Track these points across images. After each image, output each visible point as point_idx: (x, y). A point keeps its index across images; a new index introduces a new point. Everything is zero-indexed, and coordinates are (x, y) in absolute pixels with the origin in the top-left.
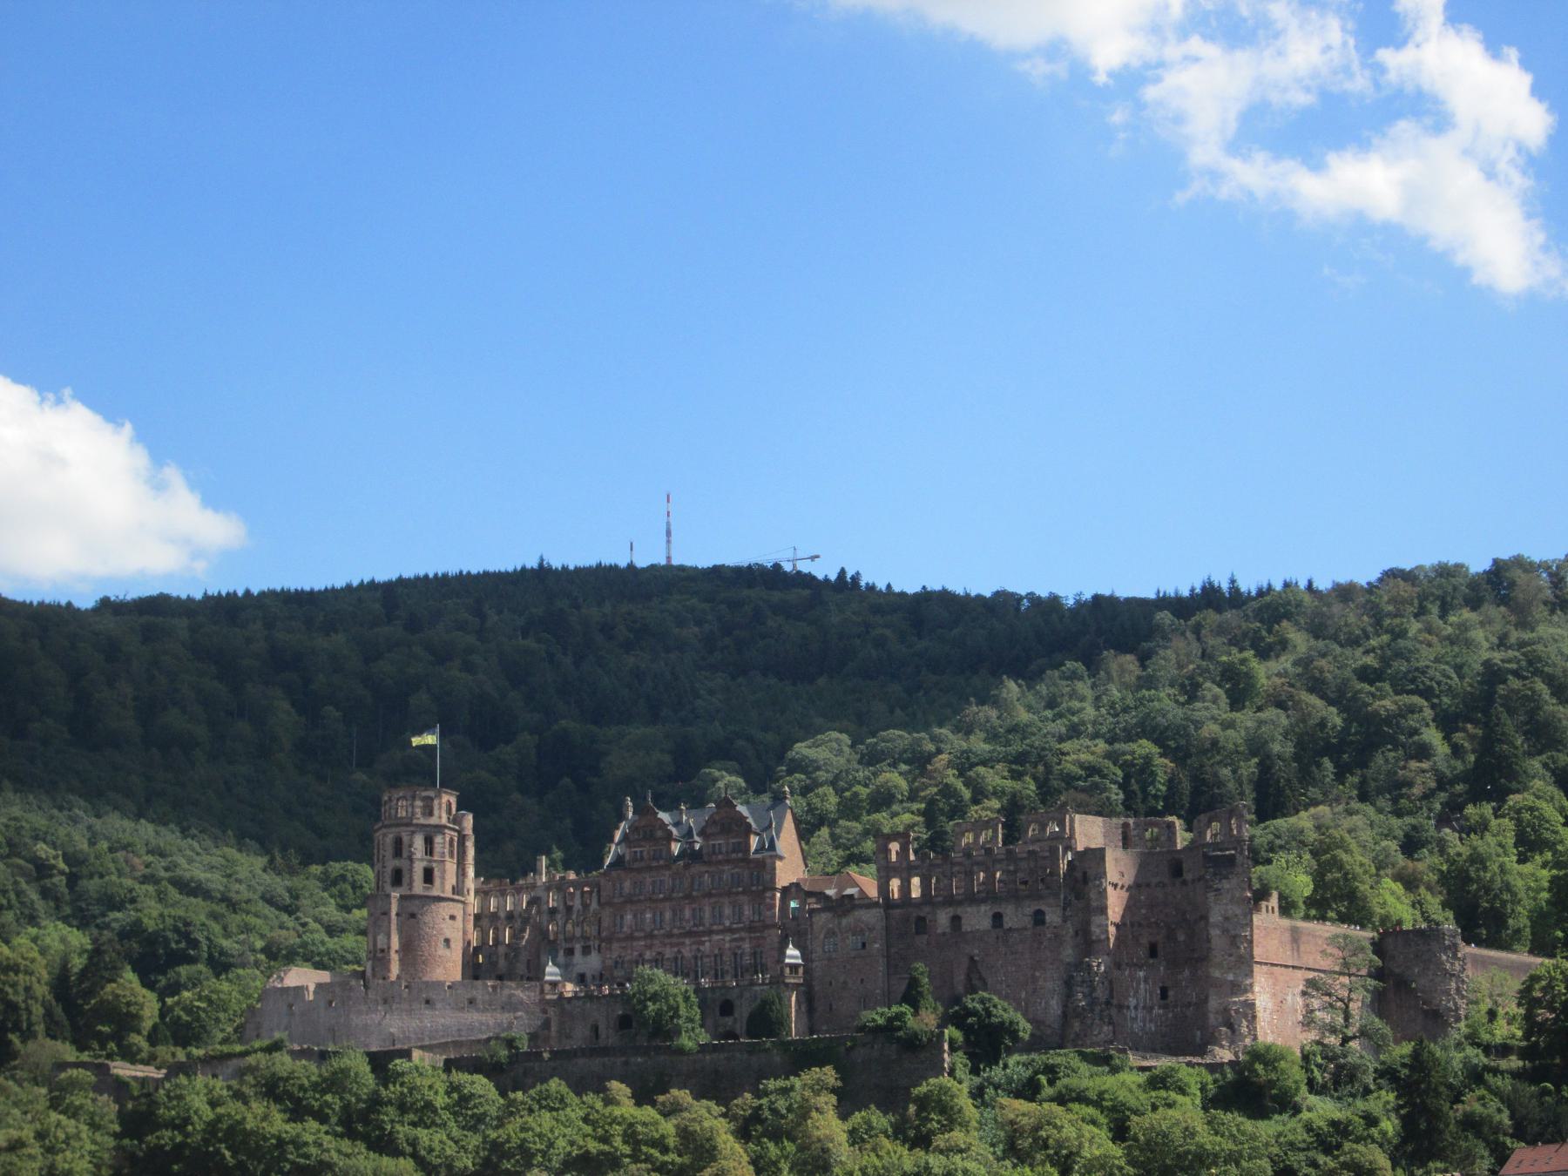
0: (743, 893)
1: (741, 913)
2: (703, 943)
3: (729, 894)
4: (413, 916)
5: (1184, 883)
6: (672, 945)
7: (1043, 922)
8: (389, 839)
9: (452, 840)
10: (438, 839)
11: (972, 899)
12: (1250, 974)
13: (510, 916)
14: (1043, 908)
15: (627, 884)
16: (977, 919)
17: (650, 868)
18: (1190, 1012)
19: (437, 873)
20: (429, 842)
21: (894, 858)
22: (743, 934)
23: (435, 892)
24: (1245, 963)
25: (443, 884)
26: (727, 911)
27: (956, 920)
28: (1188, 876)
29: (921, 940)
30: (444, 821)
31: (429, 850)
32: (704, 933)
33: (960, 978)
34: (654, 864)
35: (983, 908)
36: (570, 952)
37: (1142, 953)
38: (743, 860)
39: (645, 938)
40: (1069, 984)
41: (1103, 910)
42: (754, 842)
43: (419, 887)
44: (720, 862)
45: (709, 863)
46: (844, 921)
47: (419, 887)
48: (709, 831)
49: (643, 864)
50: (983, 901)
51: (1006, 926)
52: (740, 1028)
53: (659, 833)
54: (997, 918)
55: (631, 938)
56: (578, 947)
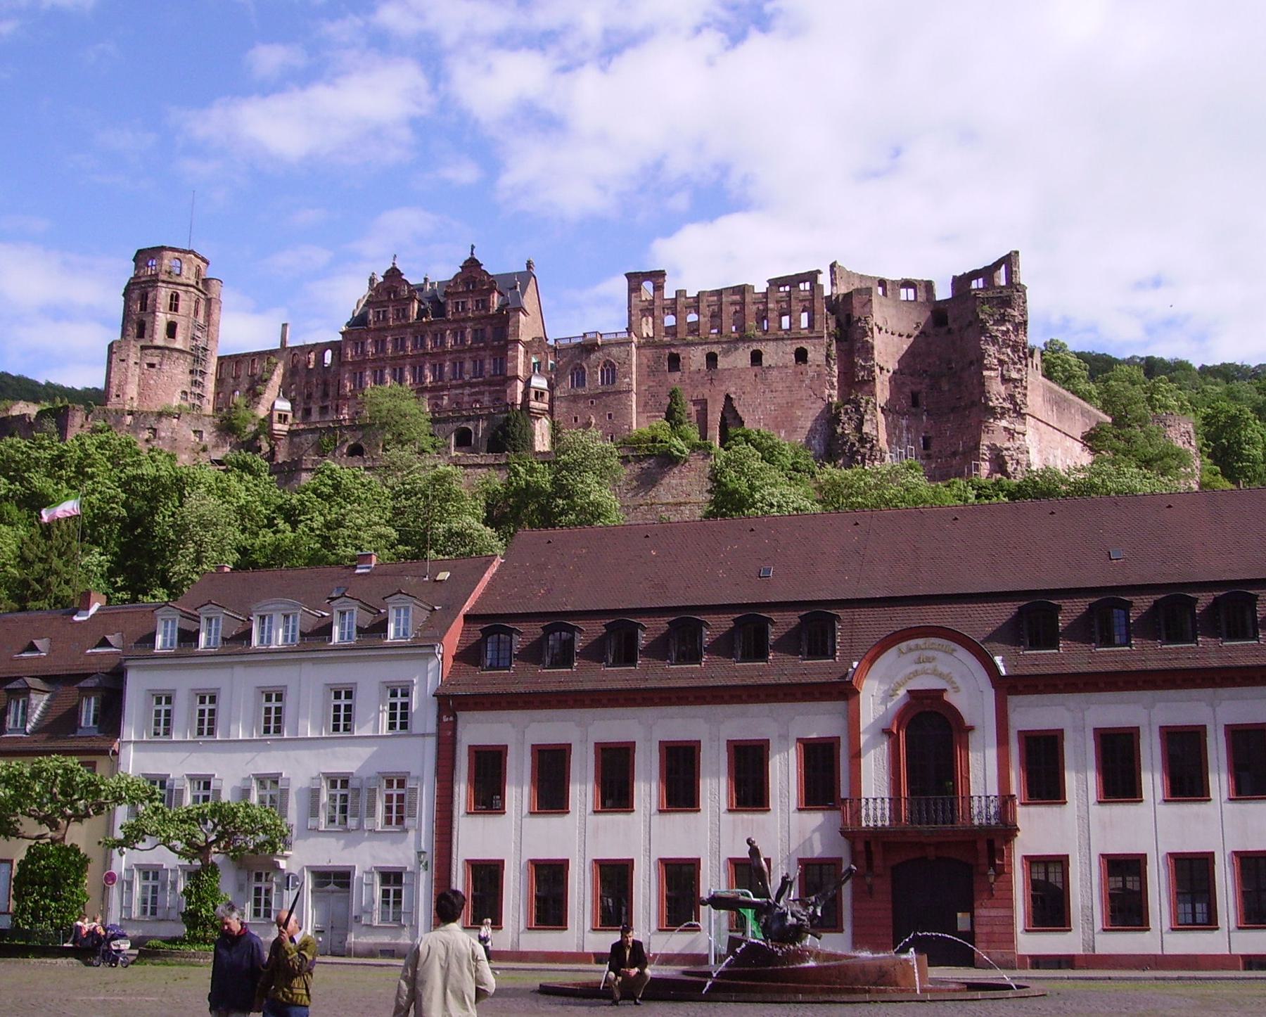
0: (483, 349)
1: (482, 369)
4: (152, 365)
7: (805, 361)
9: (197, 302)
10: (182, 295)
14: (809, 348)
19: (179, 331)
22: (482, 388)
23: (179, 343)
26: (468, 365)
28: (952, 325)
31: (174, 307)
32: (443, 388)
37: (905, 403)
38: (484, 317)
41: (868, 350)
42: (496, 300)
43: (160, 338)
44: (464, 320)
46: (593, 357)
51: (765, 364)
54: (756, 357)
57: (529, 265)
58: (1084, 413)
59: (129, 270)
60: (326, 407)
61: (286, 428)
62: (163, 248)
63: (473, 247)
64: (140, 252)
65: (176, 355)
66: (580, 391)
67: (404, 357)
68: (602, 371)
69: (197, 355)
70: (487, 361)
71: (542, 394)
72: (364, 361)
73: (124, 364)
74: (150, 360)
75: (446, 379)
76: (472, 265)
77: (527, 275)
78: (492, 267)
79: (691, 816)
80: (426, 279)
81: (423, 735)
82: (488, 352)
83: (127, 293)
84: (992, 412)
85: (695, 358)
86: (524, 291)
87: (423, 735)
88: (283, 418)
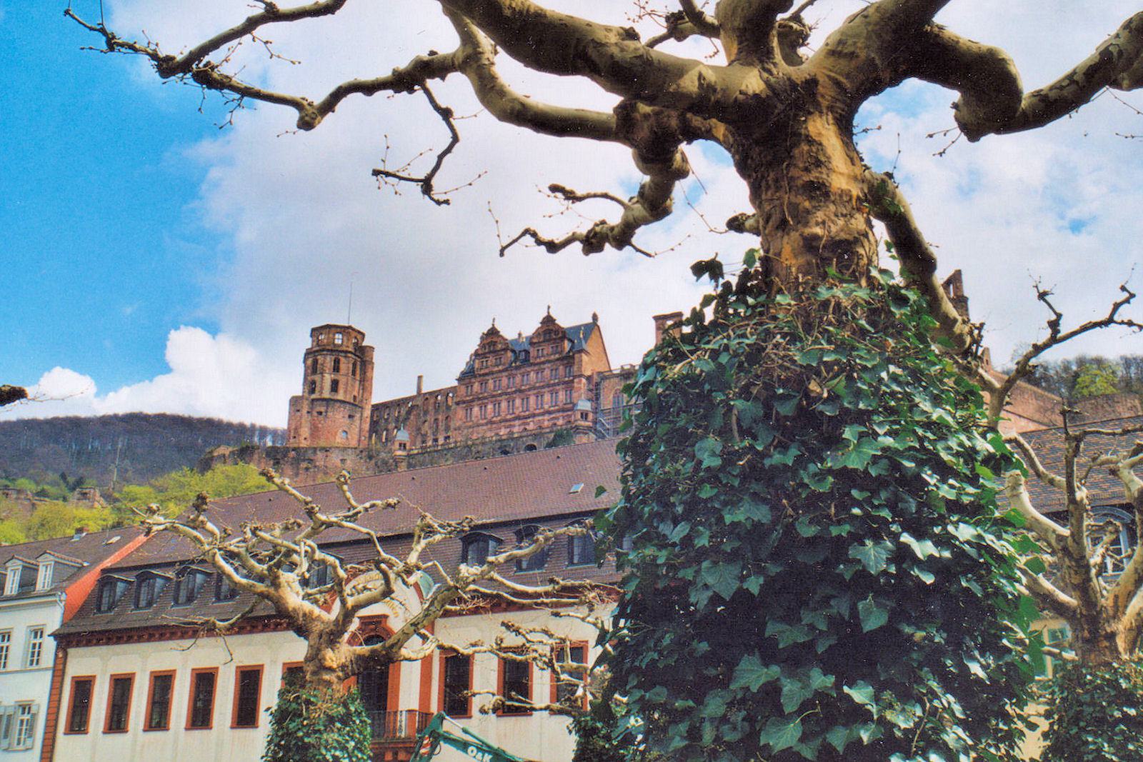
0: (558, 384)
2: (528, 424)
3: (548, 386)
4: (320, 413)
9: (354, 365)
10: (343, 360)
17: (492, 373)
20: (337, 362)
22: (558, 415)
23: (340, 396)
26: (547, 397)
30: (351, 349)
31: (336, 369)
38: (558, 360)
39: (486, 424)
44: (543, 363)
45: (535, 364)
48: (535, 341)
49: (487, 371)
57: (595, 317)
58: (1037, 397)
59: (308, 343)
61: (404, 453)
62: (328, 327)
63: (549, 307)
64: (313, 330)
65: (338, 404)
67: (500, 395)
69: (355, 405)
70: (561, 393)
71: (587, 415)
72: (473, 401)
73: (298, 414)
74: (318, 409)
75: (531, 409)
76: (548, 320)
77: (592, 328)
78: (564, 321)
79: (205, 732)
80: (520, 335)
81: (46, 669)
82: (561, 386)
83: (305, 362)
86: (586, 338)
87: (46, 669)
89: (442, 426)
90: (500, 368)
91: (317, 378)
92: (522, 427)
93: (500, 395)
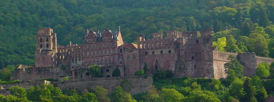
3: (108, 48)
4: (44, 54)
5: (199, 44)
6: (97, 58)
8: (39, 38)
11: (157, 48)
12: (213, 62)
13: (64, 53)
14: (171, 50)
15: (88, 46)
16: (157, 52)
17: (92, 43)
18: (201, 70)
21: (141, 40)
22: (111, 56)
23: (49, 49)
24: (211, 60)
25: (50, 47)
27: (153, 52)
29: (146, 57)
33: (154, 64)
34: (93, 42)
35: (159, 50)
36: (76, 60)
37: (191, 59)
38: (110, 41)
39: (92, 57)
40: (176, 64)
44: (106, 42)
45: (104, 42)
46: (131, 53)
47: (46, 49)
48: (104, 35)
50: (158, 49)
52: (111, 75)
53: (94, 36)
54: (162, 52)
55: (89, 57)
56: (78, 60)
60: (80, 59)
66: (129, 60)
67: (95, 50)
68: (133, 56)
72: (87, 50)
84: (206, 61)
85: (150, 53)
88: (73, 67)
89: (78, 56)
90: (94, 42)
91: (42, 43)
92: (101, 59)
93: (95, 50)
